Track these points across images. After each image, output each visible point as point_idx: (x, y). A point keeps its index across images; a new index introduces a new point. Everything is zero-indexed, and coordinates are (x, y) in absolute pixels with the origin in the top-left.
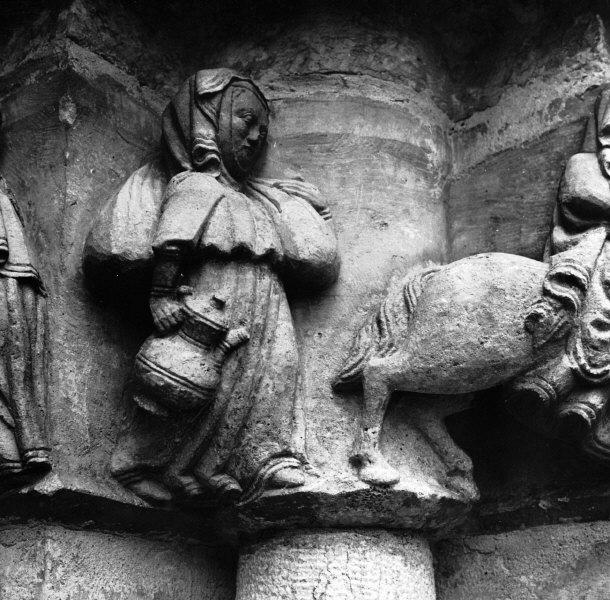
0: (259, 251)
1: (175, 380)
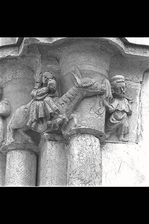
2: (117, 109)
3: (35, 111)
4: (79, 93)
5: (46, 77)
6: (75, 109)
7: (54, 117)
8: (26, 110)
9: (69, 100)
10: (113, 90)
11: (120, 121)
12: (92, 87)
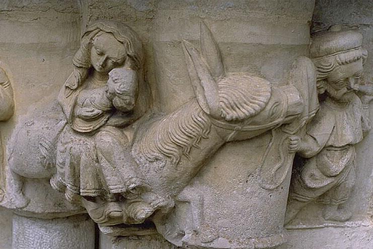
2: (330, 143)
4: (213, 133)
5: (102, 54)
6: (197, 173)
7: (128, 199)
9: (176, 152)
10: (322, 84)
11: (333, 179)
12: (257, 119)
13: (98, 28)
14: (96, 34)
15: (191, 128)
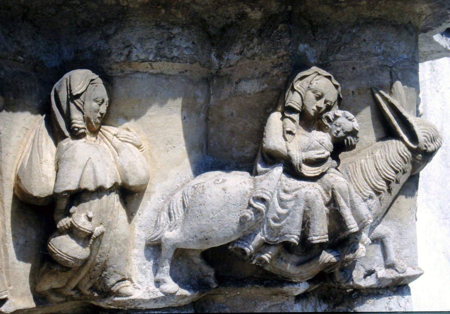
0: (108, 186)
1: (70, 259)
3: (298, 220)
5: (319, 98)
8: (260, 206)
13: (316, 72)
14: (315, 78)
15: (399, 163)
